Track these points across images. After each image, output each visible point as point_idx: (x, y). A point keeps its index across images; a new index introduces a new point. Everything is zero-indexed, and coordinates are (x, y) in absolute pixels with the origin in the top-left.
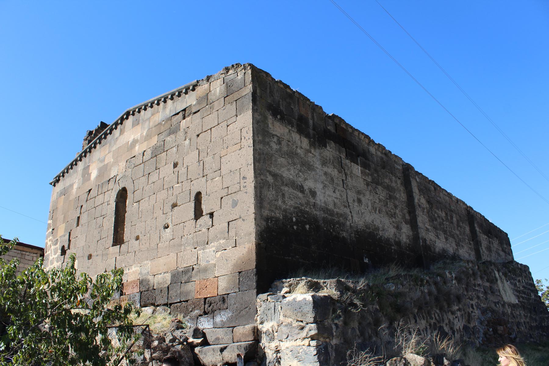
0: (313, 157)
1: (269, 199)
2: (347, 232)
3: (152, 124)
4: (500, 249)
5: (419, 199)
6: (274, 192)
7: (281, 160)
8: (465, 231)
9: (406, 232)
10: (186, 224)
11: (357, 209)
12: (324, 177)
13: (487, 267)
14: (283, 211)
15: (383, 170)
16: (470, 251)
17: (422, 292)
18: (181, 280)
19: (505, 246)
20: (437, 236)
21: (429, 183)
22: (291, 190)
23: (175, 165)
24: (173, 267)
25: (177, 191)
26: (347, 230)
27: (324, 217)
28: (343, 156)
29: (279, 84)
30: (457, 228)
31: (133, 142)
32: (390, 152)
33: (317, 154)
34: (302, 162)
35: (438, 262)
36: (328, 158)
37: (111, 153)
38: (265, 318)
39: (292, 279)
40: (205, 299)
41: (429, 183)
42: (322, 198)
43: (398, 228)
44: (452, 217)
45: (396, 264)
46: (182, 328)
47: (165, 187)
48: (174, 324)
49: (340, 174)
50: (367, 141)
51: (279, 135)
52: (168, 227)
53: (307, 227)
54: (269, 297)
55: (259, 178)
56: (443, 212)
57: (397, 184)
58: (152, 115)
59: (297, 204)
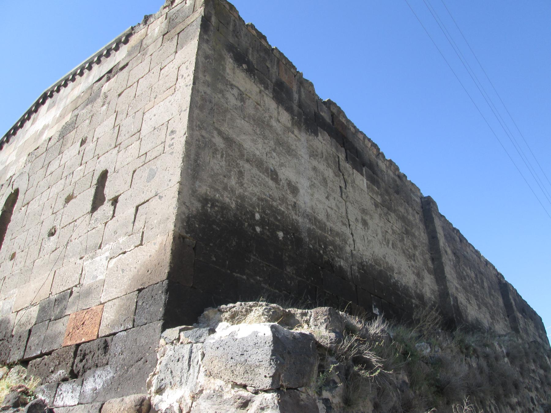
1: (212, 169)
2: (346, 260)
3: (69, 100)
4: (537, 334)
6: (223, 163)
9: (429, 283)
10: (78, 222)
11: (363, 233)
12: (312, 173)
14: (237, 198)
15: (396, 195)
17: (470, 366)
18: (51, 316)
19: (541, 332)
20: (468, 300)
21: (453, 231)
22: (255, 171)
23: (83, 142)
24: (44, 294)
25: (76, 178)
27: (309, 228)
28: (342, 156)
29: (249, 28)
30: (490, 297)
31: (43, 129)
34: (277, 139)
36: (319, 151)
37: (16, 151)
38: (167, 381)
39: (238, 303)
40: (78, 345)
41: (453, 231)
42: (307, 199)
43: (418, 275)
44: (482, 282)
46: (24, 404)
47: (64, 175)
48: (12, 396)
51: (241, 89)
52: (55, 231)
53: (281, 234)
54: (182, 334)
55: (198, 133)
56: (472, 272)
57: (416, 219)
58: (72, 90)
59: (264, 194)
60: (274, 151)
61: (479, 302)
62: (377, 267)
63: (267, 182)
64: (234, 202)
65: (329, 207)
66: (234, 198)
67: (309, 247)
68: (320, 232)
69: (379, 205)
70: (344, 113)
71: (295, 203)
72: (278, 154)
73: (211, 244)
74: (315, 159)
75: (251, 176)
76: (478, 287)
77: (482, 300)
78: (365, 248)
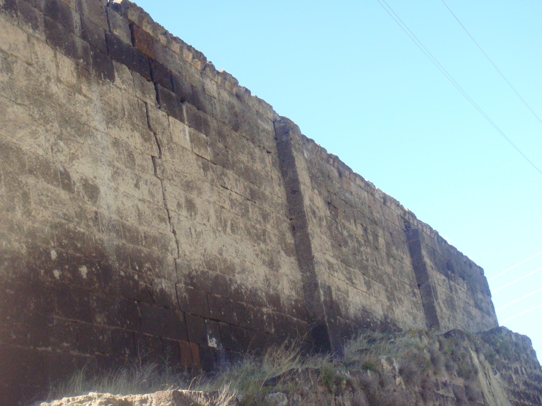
0: (86, 104)
2: (169, 279)
4: (472, 302)
5: (312, 198)
7: (16, 111)
8: (402, 267)
9: (288, 272)
12: (112, 152)
13: (457, 345)
15: (235, 134)
16: (415, 311)
19: (480, 296)
20: (350, 279)
21: (328, 162)
22: (42, 184)
26: (170, 274)
27: (118, 246)
28: (151, 100)
30: (388, 260)
32: (247, 91)
33: (95, 97)
34: (62, 115)
35: (355, 338)
36: (119, 107)
39: (65, 399)
43: (272, 264)
44: (376, 236)
45: (287, 348)
49: (147, 144)
50: (199, 65)
53: (84, 270)
56: (359, 226)
57: (265, 165)
60: (61, 139)
61: (369, 276)
62: (211, 272)
63: (58, 195)
64: (24, 245)
65: (140, 200)
66: (24, 239)
67: (119, 275)
68: (132, 246)
69: (210, 164)
70: (147, 15)
71: (96, 213)
72: (67, 141)
73: (8, 318)
74: (114, 124)
75: (39, 195)
76: (369, 250)
77: (374, 271)
78: (193, 249)
